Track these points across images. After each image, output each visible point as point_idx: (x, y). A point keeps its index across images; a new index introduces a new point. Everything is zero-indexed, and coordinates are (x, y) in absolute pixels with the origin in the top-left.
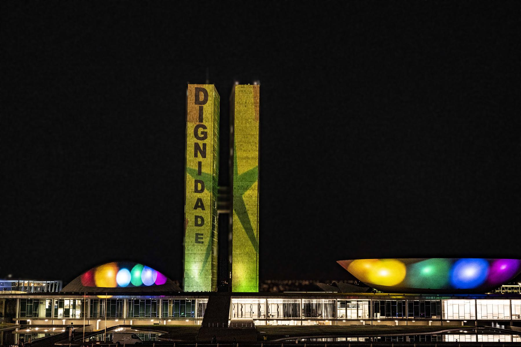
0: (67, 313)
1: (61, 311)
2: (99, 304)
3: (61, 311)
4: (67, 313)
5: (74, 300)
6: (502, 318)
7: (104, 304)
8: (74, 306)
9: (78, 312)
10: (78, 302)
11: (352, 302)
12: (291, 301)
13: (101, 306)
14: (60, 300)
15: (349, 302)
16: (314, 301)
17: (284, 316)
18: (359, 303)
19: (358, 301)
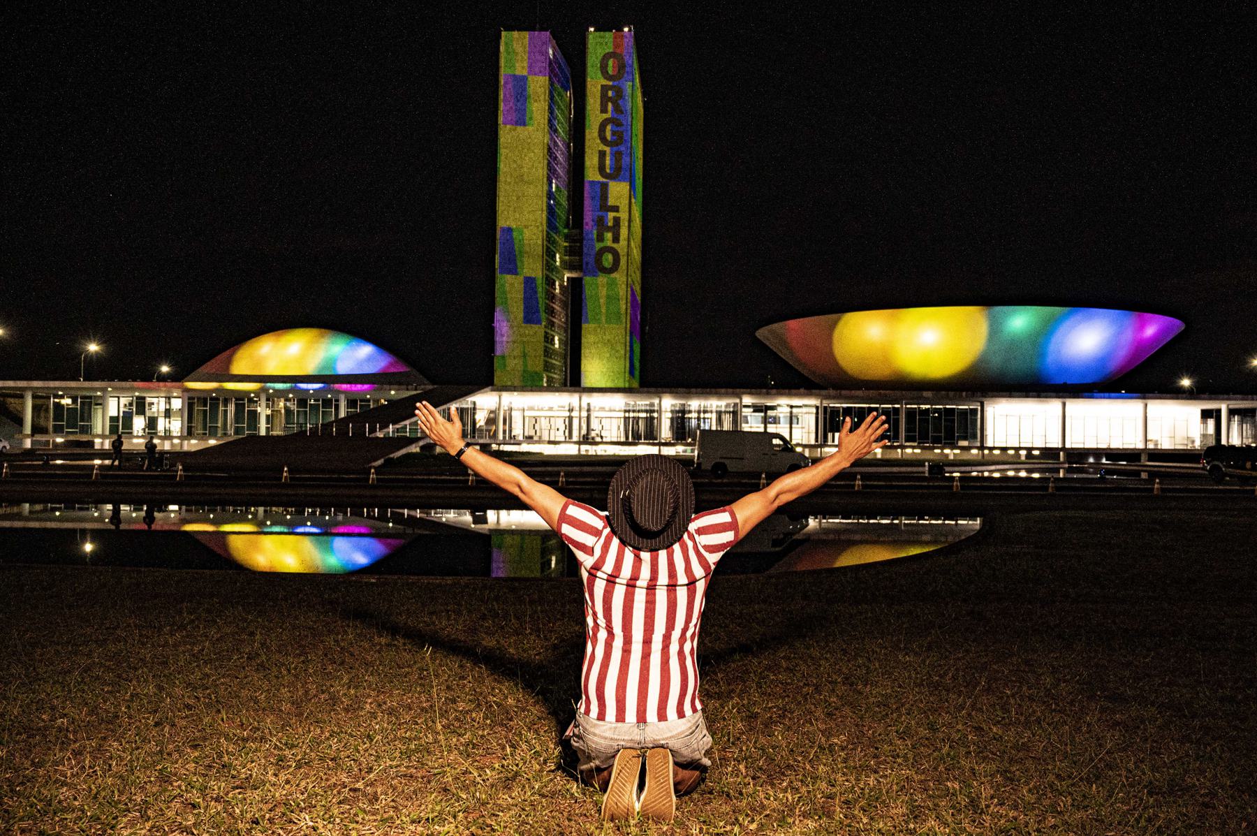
0: (152, 423)
1: (139, 423)
2: (221, 408)
3: (139, 423)
4: (152, 423)
5: (168, 399)
6: (1116, 444)
7: (231, 408)
8: (168, 413)
9: (176, 426)
10: (177, 404)
11: (779, 409)
12: (642, 402)
13: (226, 411)
14: (138, 398)
15: (773, 408)
16: (694, 404)
17: (627, 438)
18: (795, 410)
19: (792, 407)
